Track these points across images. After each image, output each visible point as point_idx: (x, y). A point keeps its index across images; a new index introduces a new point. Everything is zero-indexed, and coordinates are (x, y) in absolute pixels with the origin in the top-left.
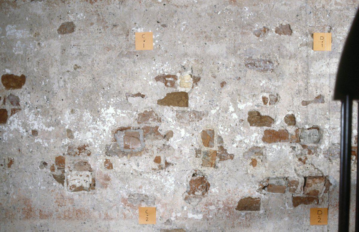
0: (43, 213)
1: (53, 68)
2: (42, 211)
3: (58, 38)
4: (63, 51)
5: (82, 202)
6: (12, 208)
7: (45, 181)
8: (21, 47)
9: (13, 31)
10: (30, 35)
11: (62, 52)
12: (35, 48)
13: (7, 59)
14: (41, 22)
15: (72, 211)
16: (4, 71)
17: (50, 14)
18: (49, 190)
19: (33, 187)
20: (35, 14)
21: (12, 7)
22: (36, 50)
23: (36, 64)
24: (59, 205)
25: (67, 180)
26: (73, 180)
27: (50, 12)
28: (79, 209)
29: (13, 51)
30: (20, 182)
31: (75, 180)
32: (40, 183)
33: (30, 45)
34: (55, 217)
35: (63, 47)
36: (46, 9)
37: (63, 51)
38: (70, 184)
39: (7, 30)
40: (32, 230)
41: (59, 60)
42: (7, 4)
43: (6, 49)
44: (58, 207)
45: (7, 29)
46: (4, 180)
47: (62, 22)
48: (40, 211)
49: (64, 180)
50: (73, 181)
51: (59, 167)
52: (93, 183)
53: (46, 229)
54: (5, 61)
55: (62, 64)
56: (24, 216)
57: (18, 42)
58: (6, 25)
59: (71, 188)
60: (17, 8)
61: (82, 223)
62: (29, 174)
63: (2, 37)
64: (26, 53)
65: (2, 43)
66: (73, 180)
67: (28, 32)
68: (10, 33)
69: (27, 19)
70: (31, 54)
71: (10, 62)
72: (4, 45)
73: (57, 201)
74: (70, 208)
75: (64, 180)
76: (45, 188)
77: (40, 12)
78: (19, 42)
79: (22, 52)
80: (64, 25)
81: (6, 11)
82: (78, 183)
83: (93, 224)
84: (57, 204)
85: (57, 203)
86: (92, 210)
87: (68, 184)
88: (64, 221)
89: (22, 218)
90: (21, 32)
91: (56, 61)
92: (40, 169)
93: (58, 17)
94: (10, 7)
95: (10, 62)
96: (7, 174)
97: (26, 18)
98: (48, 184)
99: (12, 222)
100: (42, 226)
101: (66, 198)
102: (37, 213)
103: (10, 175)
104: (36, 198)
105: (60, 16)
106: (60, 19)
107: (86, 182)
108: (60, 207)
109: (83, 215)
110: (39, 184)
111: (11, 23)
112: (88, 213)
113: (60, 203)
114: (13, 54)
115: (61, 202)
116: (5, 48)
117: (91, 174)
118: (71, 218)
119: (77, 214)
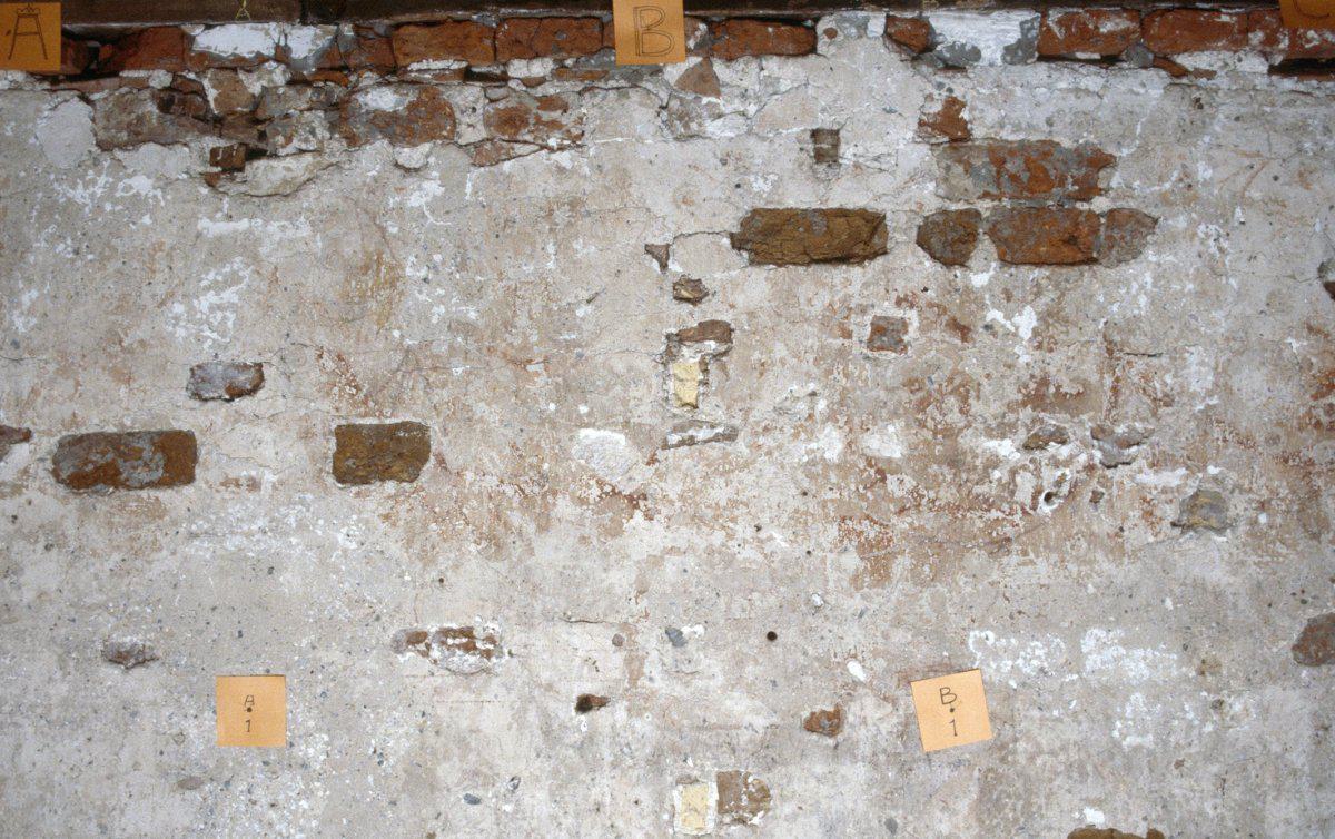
1: (1283, 803)
3: (1298, 680)
4: (1320, 733)
8: (1149, 718)
9: (1111, 653)
10: (1184, 669)
11: (1317, 735)
12: (1203, 722)
13: (1089, 768)
14: (1226, 616)
16: (1077, 815)
17: (1259, 585)
20: (1199, 586)
21: (1106, 556)
22: (1209, 728)
23: (1212, 788)
27: (1261, 577)
29: (1116, 734)
33: (1183, 709)
35: (1320, 716)
36: (1242, 563)
37: (1320, 733)
39: (1085, 650)
41: (1306, 768)
42: (1085, 545)
43: (1085, 726)
45: (1088, 644)
47: (1311, 613)
54: (1081, 775)
55: (1319, 786)
57: (1132, 697)
58: (1083, 627)
60: (1126, 560)
63: (1067, 680)
64: (1165, 743)
65: (1069, 704)
67: (1175, 657)
68: (1099, 662)
69: (1169, 603)
70: (1190, 745)
71: (1103, 778)
72: (1078, 708)
77: (1218, 575)
78: (1138, 698)
79: (1151, 737)
80: (1320, 627)
81: (1080, 572)
90: (1145, 658)
91: (1294, 772)
93: (1294, 594)
94: (1100, 556)
95: (1103, 778)
97: (1163, 601)
105: (1303, 592)
106: (1304, 602)
111: (1101, 621)
114: (1116, 744)
116: (1080, 723)
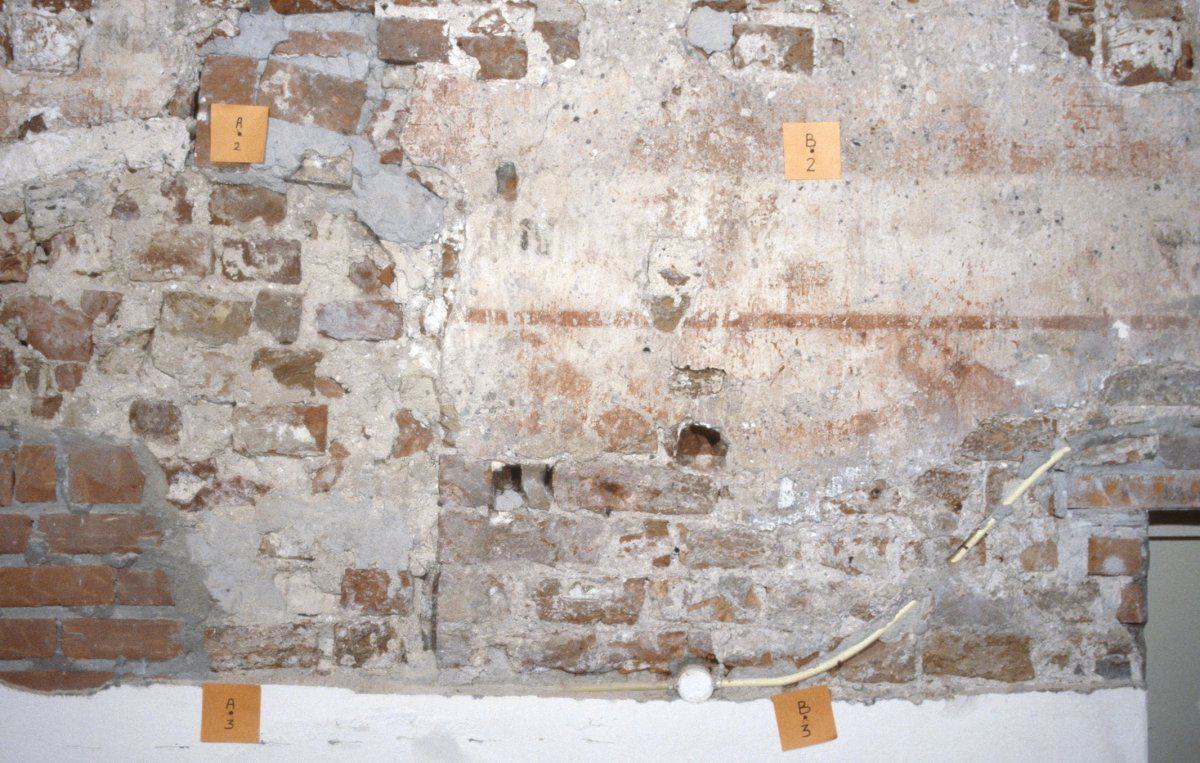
0: (1024, 153)
2: (1020, 147)
5: (1150, 119)
6: (920, 135)
7: (1033, 45)
15: (1118, 147)
18: (1047, 76)
19: (992, 67)
24: (1076, 127)
25: (1105, 45)
26: (1122, 46)
28: (1140, 143)
30: (951, 49)
31: (1129, 44)
32: (1018, 52)
34: (1064, 166)
38: (1115, 59)
40: (984, 209)
44: (1073, 132)
46: (897, 42)
48: (1015, 145)
49: (1093, 49)
50: (1124, 49)
51: (1076, 5)
52: (1185, 58)
53: (1032, 206)
56: (960, 162)
59: (1118, 70)
61: (1148, 188)
62: (980, 22)
66: (1122, 46)
73: (1069, 115)
74: (1114, 137)
75: (1093, 49)
76: (1032, 68)
82: (1139, 57)
83: (1182, 191)
84: (1072, 121)
85: (1069, 121)
86: (1181, 143)
87: (1106, 58)
88: (1094, 180)
89: (952, 167)
92: (1017, 7)
96: (909, 22)
98: (1045, 57)
99: (917, 183)
100: (1017, 198)
101: (1099, 104)
102: (1005, 154)
103: (916, 25)
104: (1001, 102)
107: (1165, 50)
108: (1080, 134)
109: (1155, 160)
110: (1015, 55)
112: (1169, 153)
113: (1080, 120)
115: (1083, 116)
117: (1178, 28)
118: (1115, 169)
119: (1134, 157)
